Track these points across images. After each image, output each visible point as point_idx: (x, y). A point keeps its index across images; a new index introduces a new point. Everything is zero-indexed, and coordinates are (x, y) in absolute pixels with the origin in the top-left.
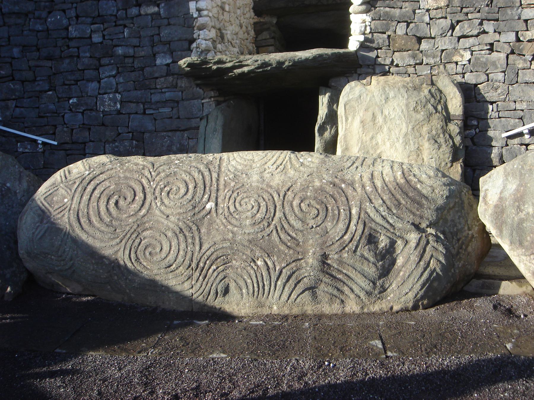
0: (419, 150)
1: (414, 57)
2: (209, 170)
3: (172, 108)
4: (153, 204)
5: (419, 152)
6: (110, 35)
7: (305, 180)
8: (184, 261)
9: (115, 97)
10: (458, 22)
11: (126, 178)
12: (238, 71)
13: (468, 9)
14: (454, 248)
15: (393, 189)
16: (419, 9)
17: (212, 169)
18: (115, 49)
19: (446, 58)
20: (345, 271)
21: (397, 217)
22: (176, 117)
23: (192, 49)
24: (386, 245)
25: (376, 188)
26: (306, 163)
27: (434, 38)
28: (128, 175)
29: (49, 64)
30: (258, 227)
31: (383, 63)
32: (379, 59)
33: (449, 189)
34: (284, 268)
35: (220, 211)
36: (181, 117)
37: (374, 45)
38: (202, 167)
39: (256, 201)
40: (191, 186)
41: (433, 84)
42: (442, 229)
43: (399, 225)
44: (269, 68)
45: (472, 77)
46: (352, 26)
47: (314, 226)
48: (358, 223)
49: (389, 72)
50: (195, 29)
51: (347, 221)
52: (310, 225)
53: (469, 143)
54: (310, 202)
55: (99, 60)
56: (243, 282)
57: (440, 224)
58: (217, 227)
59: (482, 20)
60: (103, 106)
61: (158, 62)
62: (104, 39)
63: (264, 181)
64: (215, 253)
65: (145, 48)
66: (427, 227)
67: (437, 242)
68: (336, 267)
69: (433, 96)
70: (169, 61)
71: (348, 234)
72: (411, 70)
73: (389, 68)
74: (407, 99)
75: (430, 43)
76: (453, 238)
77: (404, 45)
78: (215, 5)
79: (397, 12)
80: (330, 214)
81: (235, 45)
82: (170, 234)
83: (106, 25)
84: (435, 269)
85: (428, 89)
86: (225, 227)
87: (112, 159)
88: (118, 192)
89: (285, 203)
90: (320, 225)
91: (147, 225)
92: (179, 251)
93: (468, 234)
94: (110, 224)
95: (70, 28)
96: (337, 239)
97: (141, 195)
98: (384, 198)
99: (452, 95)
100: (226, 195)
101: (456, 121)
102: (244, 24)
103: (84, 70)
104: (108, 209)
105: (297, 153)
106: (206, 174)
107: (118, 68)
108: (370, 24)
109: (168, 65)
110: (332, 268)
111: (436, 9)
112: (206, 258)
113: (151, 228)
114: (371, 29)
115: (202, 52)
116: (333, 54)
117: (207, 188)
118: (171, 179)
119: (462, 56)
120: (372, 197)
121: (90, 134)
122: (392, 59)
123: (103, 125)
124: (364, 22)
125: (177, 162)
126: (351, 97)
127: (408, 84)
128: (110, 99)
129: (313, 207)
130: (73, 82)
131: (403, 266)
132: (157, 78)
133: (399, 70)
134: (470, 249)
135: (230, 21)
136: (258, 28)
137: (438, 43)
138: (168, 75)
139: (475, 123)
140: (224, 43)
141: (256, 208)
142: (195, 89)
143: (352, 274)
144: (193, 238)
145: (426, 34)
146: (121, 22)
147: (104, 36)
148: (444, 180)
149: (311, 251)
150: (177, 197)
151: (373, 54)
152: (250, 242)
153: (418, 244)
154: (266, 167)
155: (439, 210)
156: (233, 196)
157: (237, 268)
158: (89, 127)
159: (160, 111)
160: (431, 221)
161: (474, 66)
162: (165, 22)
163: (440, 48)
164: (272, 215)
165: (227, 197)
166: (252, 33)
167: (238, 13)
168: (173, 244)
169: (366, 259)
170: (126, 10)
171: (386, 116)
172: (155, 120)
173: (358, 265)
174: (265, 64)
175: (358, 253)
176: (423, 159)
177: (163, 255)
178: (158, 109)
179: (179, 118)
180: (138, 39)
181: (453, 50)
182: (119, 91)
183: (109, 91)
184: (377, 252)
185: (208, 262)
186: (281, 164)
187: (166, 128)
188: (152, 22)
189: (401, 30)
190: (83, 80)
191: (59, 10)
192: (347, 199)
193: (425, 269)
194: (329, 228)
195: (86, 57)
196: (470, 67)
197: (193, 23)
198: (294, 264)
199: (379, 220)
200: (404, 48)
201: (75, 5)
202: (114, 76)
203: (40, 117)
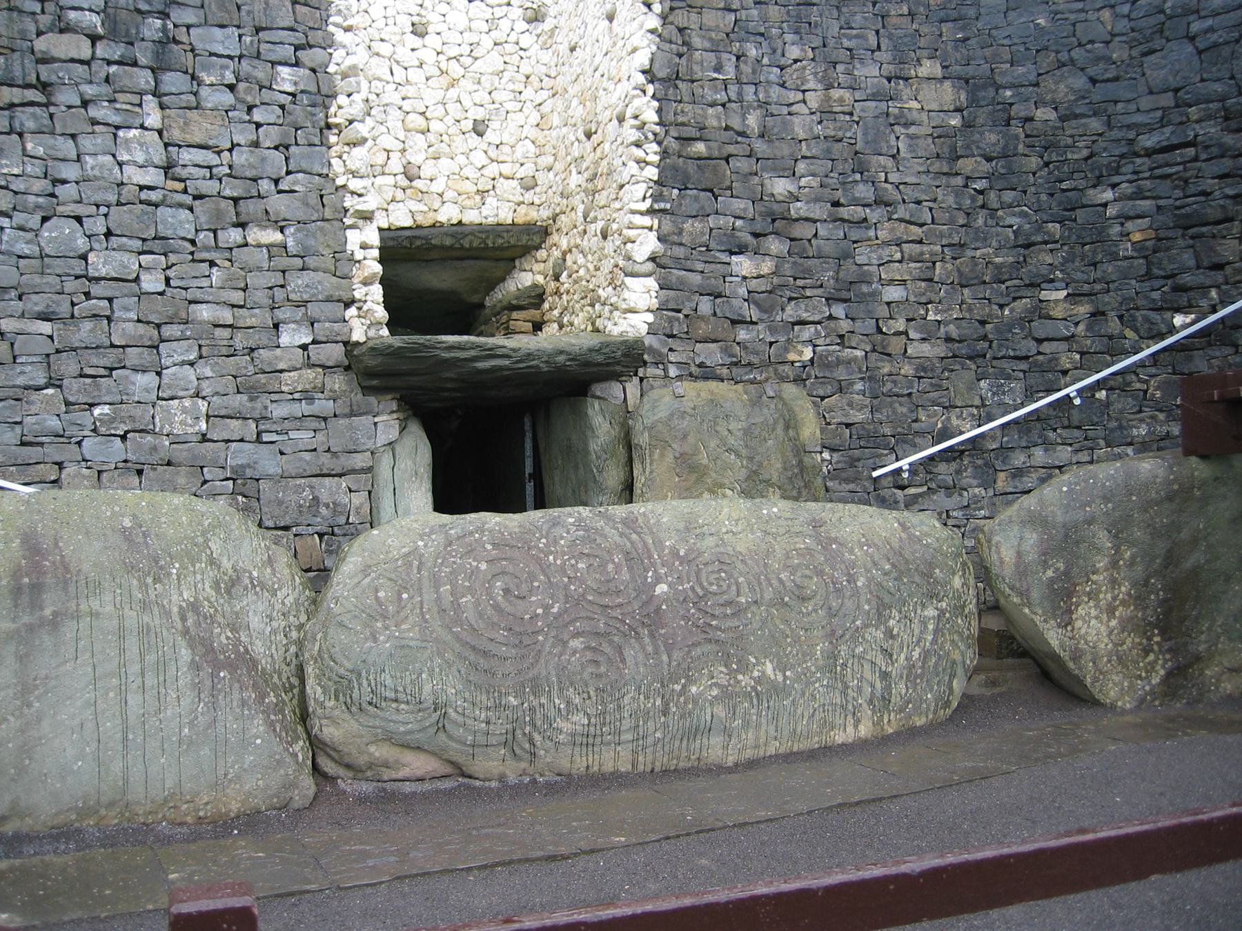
10: (791, 299)
27: (756, 323)
29: (46, 328)
50: (355, 280)
59: (827, 299)
61: (285, 339)
65: (257, 311)
70: (308, 340)
83: (173, 258)
95: (92, 257)
107: (200, 346)
109: (304, 347)
123: (169, 464)
125: (571, 520)
128: (185, 411)
130: (102, 372)
132: (281, 371)
141: (734, 588)
147: (168, 280)
158: (139, 467)
170: (215, 232)
172: (282, 453)
180: (241, 293)
182: (204, 394)
183: (181, 394)
188: (270, 258)
189: (705, 306)
190: (124, 367)
191: (68, 216)
195: (129, 320)
201: (103, 210)
202: (192, 364)
203: (23, 444)
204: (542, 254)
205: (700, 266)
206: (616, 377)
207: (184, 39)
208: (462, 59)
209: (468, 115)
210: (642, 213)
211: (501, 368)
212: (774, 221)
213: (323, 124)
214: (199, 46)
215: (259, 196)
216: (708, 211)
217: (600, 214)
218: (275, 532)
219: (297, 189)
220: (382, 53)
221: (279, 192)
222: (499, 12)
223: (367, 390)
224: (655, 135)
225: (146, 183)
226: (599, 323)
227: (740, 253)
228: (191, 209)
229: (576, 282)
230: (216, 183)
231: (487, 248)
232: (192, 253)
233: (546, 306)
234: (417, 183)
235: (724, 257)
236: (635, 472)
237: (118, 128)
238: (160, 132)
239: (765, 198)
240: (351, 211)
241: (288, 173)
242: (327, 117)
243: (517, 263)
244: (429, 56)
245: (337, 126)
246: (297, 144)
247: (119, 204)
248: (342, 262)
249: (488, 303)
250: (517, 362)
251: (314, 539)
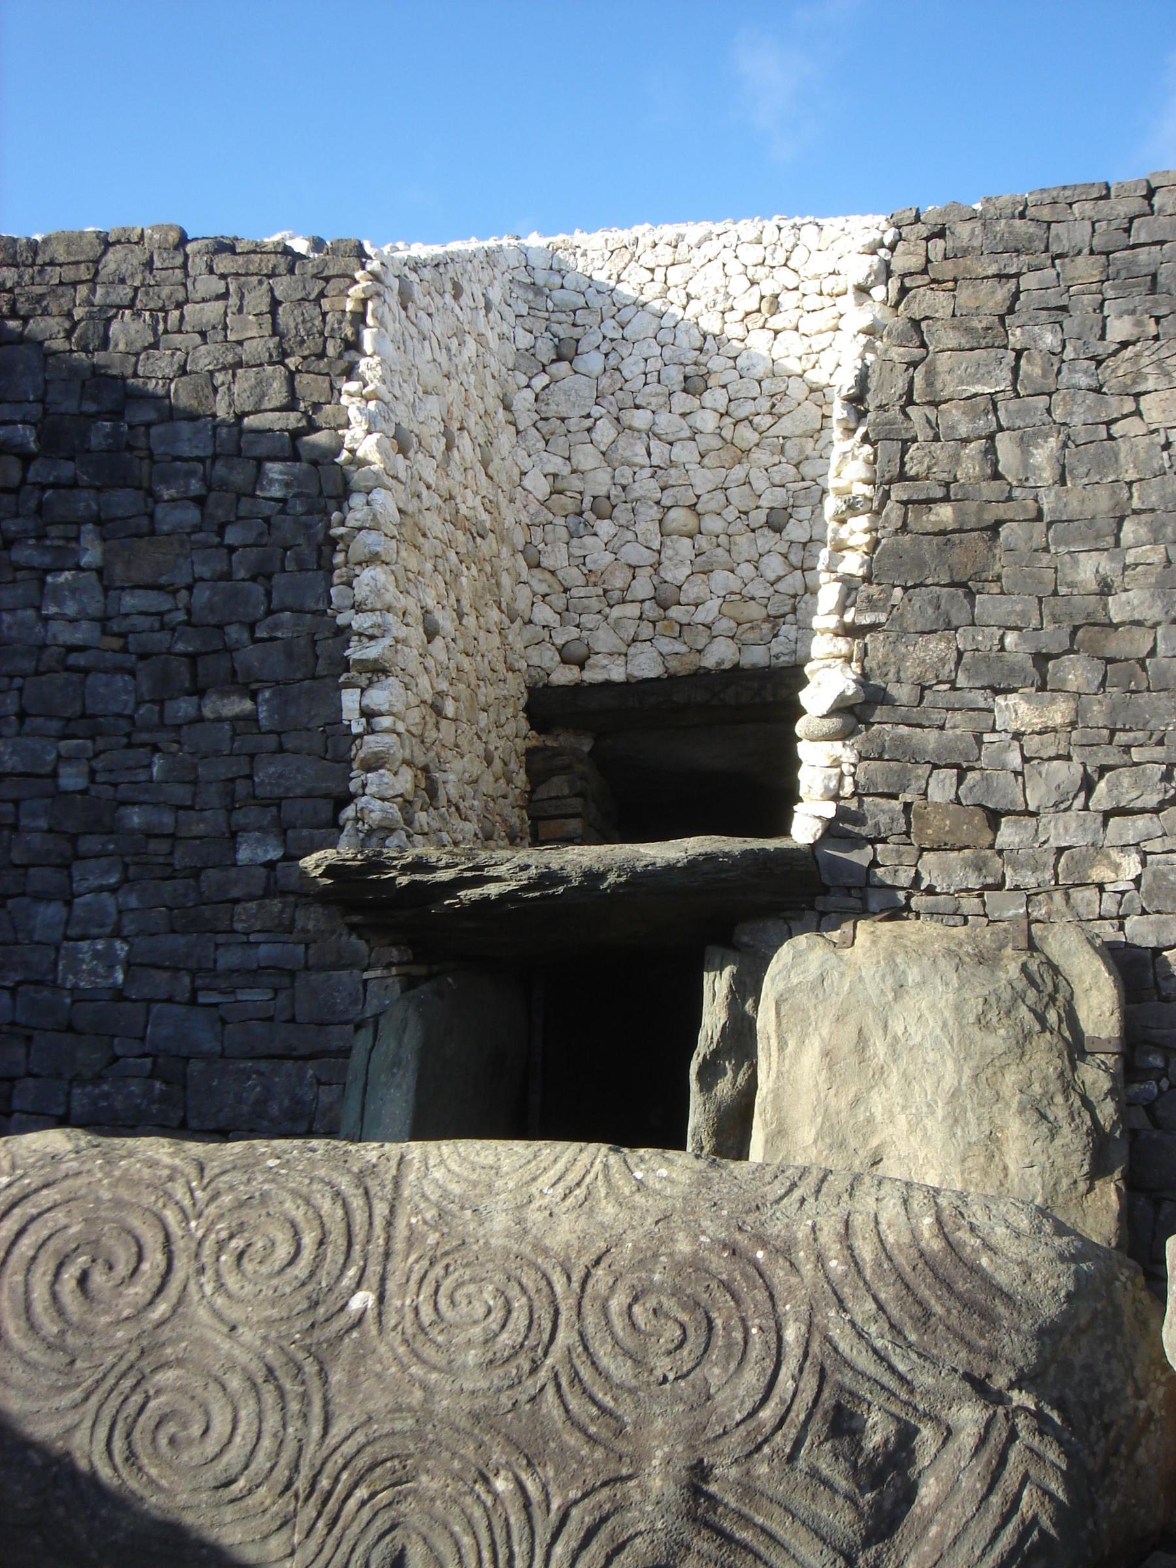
0: (992, 1142)
1: (979, 866)
2: (367, 1193)
3: (276, 991)
4: (193, 1288)
5: (992, 1147)
6: (111, 771)
7: (649, 1235)
8: (272, 1469)
9: (110, 948)
10: (1103, 770)
11: (118, 1203)
12: (473, 893)
13: (1131, 734)
14: (1094, 1454)
15: (908, 1269)
16: (994, 731)
17: (374, 1189)
18: (124, 811)
19: (1071, 873)
20: (759, 1520)
21: (920, 1355)
22: (286, 1015)
23: (341, 822)
24: (887, 1441)
25: (856, 1264)
26: (651, 1182)
28: (125, 1194)
30: (500, 1372)
31: (889, 882)
32: (880, 871)
33: (1076, 1272)
34: (576, 1502)
35: (391, 1320)
36: (298, 1018)
37: (864, 831)
38: (345, 1183)
39: (500, 1292)
40: (309, 1239)
41: (1032, 946)
42: (1055, 1394)
43: (925, 1380)
44: (561, 889)
45: (1145, 929)
46: (803, 775)
47: (671, 1376)
48: (801, 1370)
49: (907, 908)
50: (355, 765)
51: (769, 1364)
52: (659, 1373)
53: (1140, 1119)
54: (659, 1302)
55: (74, 839)
56: (449, 1542)
57: (1049, 1379)
58: (379, 1368)
60: (75, 975)
61: (244, 854)
62: (92, 781)
63: (526, 1232)
64: (369, 1449)
65: (207, 813)
66: (1012, 1386)
67: (1042, 1433)
68: (733, 1504)
69: (1032, 982)
70: (275, 854)
71: (772, 1403)
72: (970, 904)
73: (908, 898)
74: (959, 989)
75: (1026, 827)
76: (1090, 1422)
77: (951, 832)
78: (414, 701)
79: (930, 738)
80: (719, 1341)
81: (469, 812)
82: (235, 1383)
83: (101, 743)
84: (1035, 1518)
85: (1020, 962)
86: (404, 1368)
87: (83, 1143)
88: (92, 1245)
89: (586, 1302)
90: (689, 1372)
91: (169, 1351)
92: (258, 1439)
93: (1136, 1409)
94: (58, 1342)
96: (738, 1417)
97: (159, 1258)
98: (882, 1296)
99: (1088, 979)
100: (411, 1270)
101: (1102, 1057)
102: (496, 754)
103: (26, 867)
104: (54, 1296)
105: (626, 1150)
106: (357, 1203)
107: (126, 866)
109: (270, 865)
110: (720, 1510)
111: (1040, 733)
112: (341, 1462)
113: (180, 1362)
114: (856, 784)
115: (371, 832)
116: (745, 853)
117: (357, 1248)
118: (250, 1215)
119: (1117, 867)
120: (847, 1291)
121: (28, 1054)
122: (917, 873)
123: (70, 1028)
124: (836, 763)
125: (272, 1163)
126: (795, 981)
127: (960, 945)
128: (96, 955)
129: (667, 1316)
131: (938, 1508)
132: (236, 901)
133: (936, 905)
134: (1141, 1455)
135: (457, 746)
136: (539, 766)
137: (1046, 829)
138: (268, 893)
139: (1157, 1061)
140: (436, 809)
142: (344, 938)
143: (783, 1528)
144: (305, 1398)
145: (1012, 802)
146: (145, 737)
147: (92, 773)
148: (1060, 1242)
149: (659, 1453)
150: (264, 1269)
151: (861, 857)
152: (475, 1417)
153: (983, 1441)
154: (534, 1190)
155: (1044, 1333)
156: (431, 1276)
157: (433, 1500)
160: (1021, 1369)
161: (1149, 895)
162: (271, 741)
163: (1053, 843)
164: (546, 1337)
165: (415, 1277)
166: (521, 778)
167: (482, 724)
168: (243, 1413)
169: (826, 1483)
170: (161, 702)
171: (896, 1039)
173: (800, 1501)
174: (549, 878)
175: (801, 1464)
176: (1005, 1168)
177: (211, 1447)
178: (233, 992)
179: (292, 1020)
180: (189, 788)
181: (1091, 850)
182: (125, 932)
183: (95, 931)
184: (860, 1461)
185: (344, 1476)
186: (578, 1185)
188: (233, 740)
189: (942, 787)
190: (23, 894)
192: (771, 1297)
193: (1006, 1519)
194: (714, 1383)
196: (1139, 900)
198: (605, 1492)
199: (865, 1361)
200: (950, 839)
201: (18, 682)
202: (113, 890)
205: (936, 716)
207: (141, 442)
208: (756, 419)
209: (763, 502)
210: (837, 635)
212: (1076, 629)
213: (321, 537)
214: (159, 450)
215: (228, 650)
216: (955, 623)
219: (279, 635)
220: (637, 424)
221: (255, 641)
222: (819, 342)
224: (871, 500)
225: (75, 642)
227: (1014, 690)
228: (132, 673)
230: (164, 637)
232: (128, 735)
234: (675, 612)
235: (979, 699)
237: (47, 571)
238: (100, 571)
239: (1063, 590)
241: (270, 612)
242: (329, 526)
244: (707, 421)
245: (341, 536)
246: (283, 570)
247: (37, 673)
250: (524, 888)
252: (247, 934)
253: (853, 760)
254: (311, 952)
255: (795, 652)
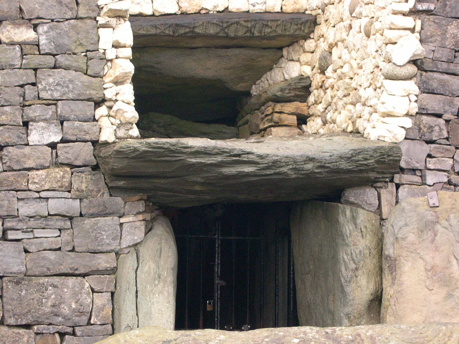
3: (60, 230)
23: (97, 118)
50: (106, 79)
65: (7, 109)
70: (57, 138)
108: (416, 99)
109: (53, 146)
132: (29, 169)
159: (36, 236)
162: (50, 60)
172: (26, 251)
178: (32, 231)
187: (48, 269)
197: (104, 68)
204: (309, 44)
206: (372, 183)
210: (404, 15)
211: (248, 175)
217: (366, 10)
218: (16, 330)
223: (113, 191)
226: (360, 124)
229: (340, 78)
231: (253, 37)
233: (311, 99)
236: (386, 283)
240: (105, 10)
243: (285, 52)
248: (93, 61)
249: (254, 91)
250: (264, 169)
251: (54, 339)
252: (38, 192)
253: (417, 93)
254: (84, 204)
255: (265, 3)
